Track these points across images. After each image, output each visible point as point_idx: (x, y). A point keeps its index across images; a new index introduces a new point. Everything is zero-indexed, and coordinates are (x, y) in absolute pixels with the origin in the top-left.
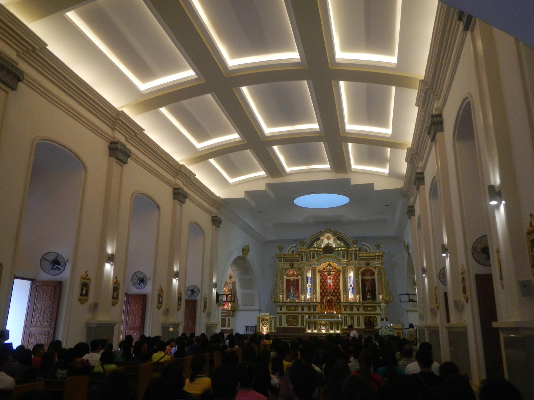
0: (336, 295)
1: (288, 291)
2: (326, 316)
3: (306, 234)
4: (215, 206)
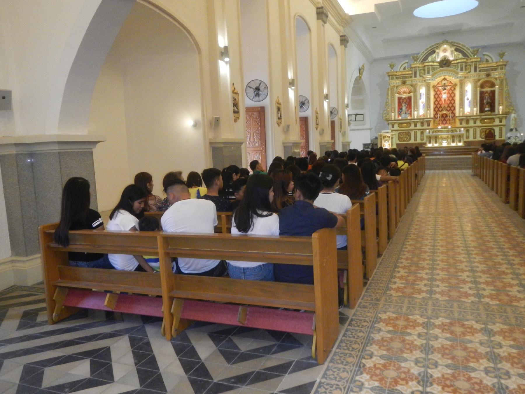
2: (440, 131)
3: (420, 49)
4: (342, 24)
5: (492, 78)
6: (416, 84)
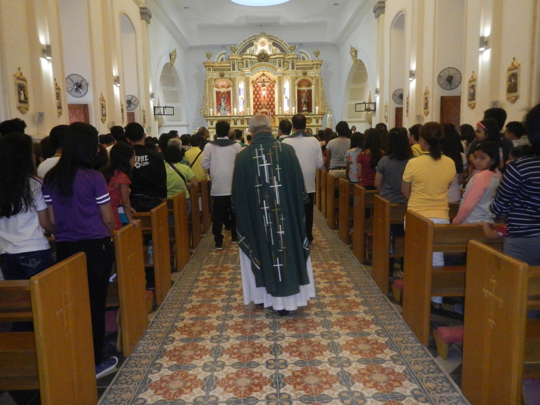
0: (270, 107)
1: (219, 104)
3: (238, 40)
6: (235, 78)
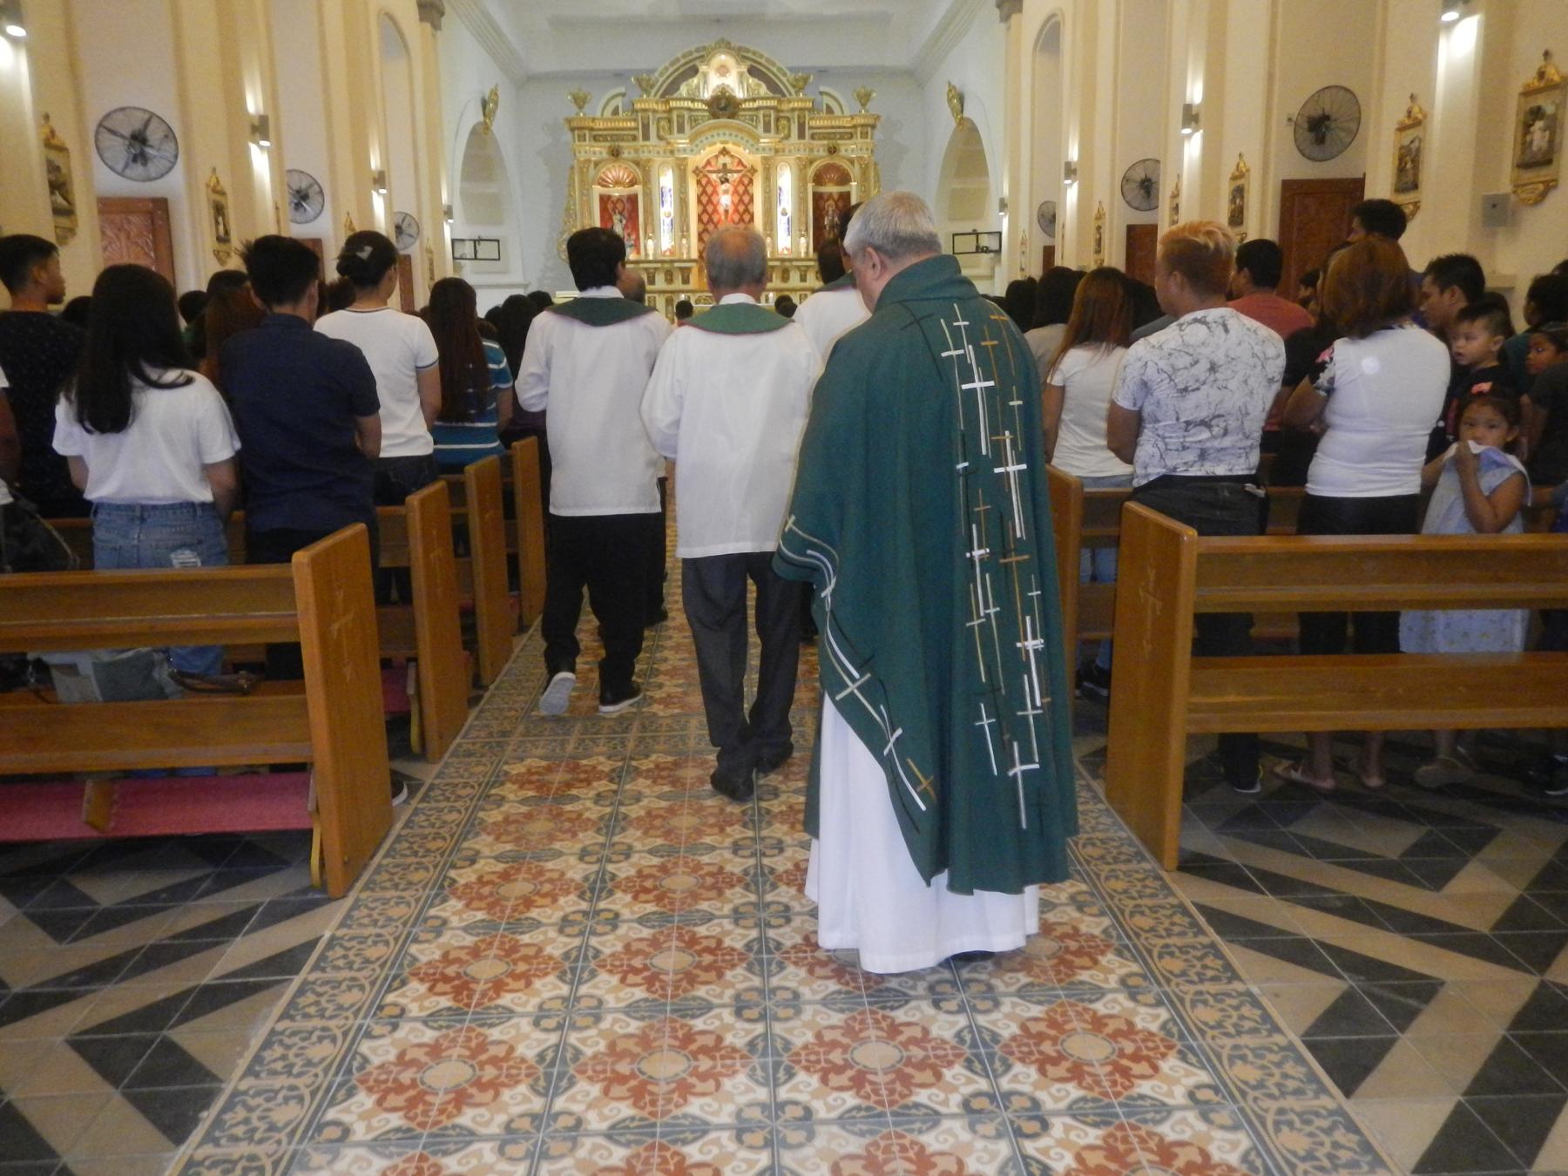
3: (658, 57)
5: (843, 158)
6: (649, 160)
